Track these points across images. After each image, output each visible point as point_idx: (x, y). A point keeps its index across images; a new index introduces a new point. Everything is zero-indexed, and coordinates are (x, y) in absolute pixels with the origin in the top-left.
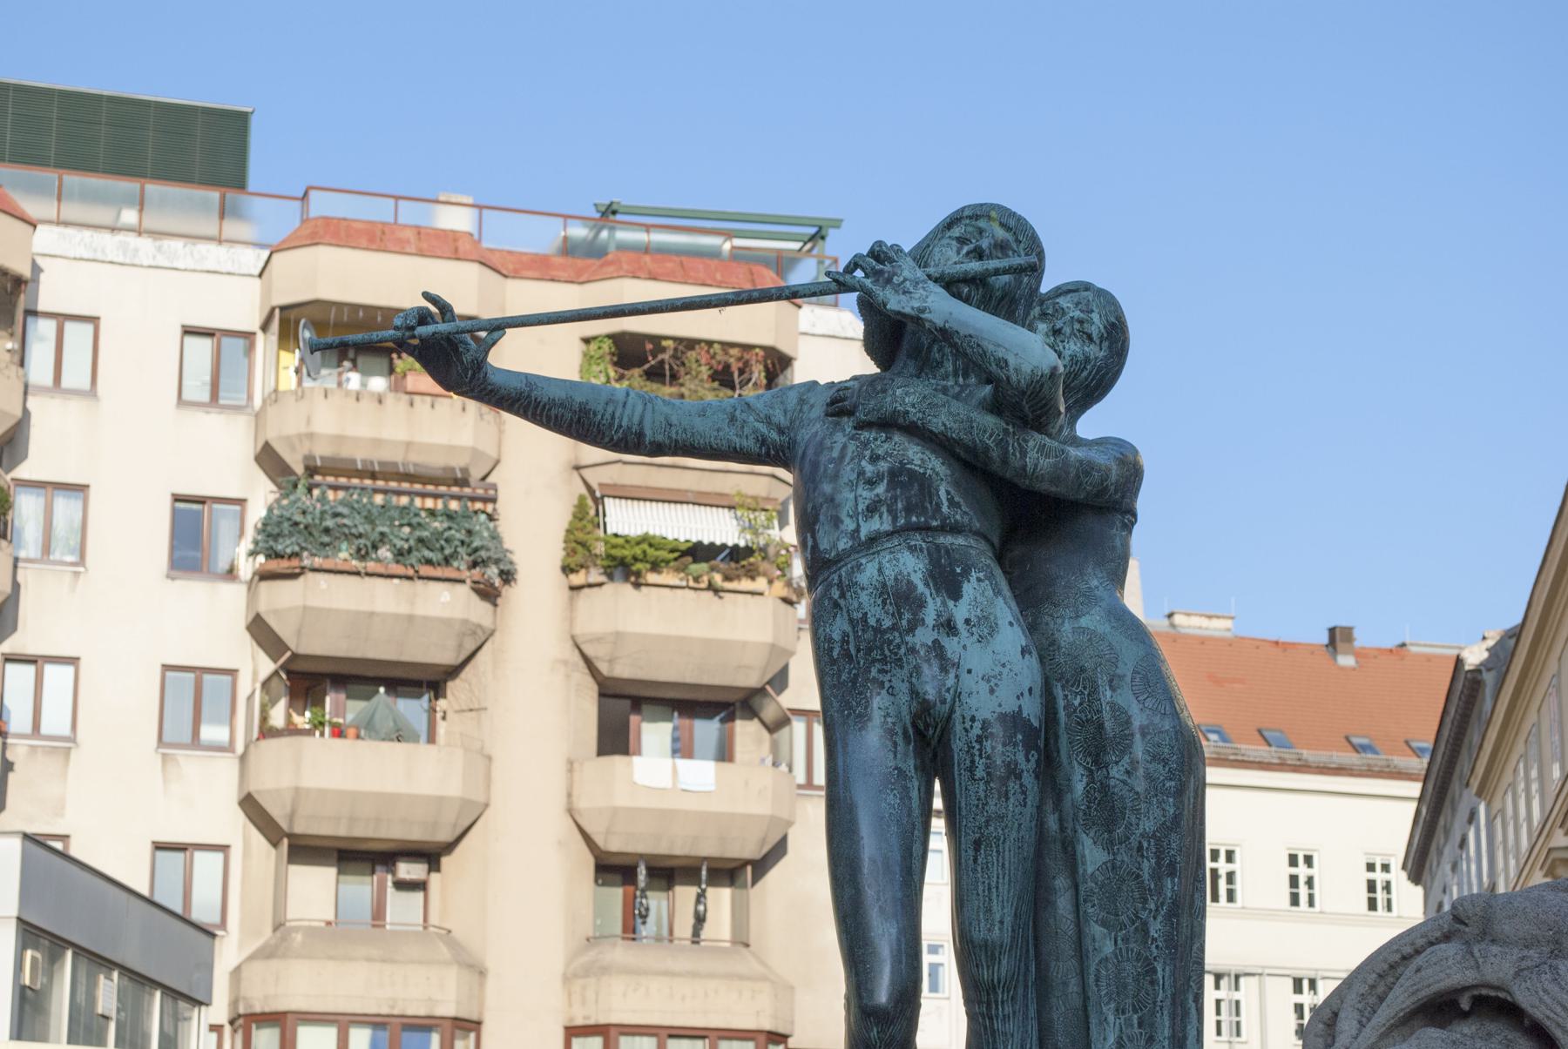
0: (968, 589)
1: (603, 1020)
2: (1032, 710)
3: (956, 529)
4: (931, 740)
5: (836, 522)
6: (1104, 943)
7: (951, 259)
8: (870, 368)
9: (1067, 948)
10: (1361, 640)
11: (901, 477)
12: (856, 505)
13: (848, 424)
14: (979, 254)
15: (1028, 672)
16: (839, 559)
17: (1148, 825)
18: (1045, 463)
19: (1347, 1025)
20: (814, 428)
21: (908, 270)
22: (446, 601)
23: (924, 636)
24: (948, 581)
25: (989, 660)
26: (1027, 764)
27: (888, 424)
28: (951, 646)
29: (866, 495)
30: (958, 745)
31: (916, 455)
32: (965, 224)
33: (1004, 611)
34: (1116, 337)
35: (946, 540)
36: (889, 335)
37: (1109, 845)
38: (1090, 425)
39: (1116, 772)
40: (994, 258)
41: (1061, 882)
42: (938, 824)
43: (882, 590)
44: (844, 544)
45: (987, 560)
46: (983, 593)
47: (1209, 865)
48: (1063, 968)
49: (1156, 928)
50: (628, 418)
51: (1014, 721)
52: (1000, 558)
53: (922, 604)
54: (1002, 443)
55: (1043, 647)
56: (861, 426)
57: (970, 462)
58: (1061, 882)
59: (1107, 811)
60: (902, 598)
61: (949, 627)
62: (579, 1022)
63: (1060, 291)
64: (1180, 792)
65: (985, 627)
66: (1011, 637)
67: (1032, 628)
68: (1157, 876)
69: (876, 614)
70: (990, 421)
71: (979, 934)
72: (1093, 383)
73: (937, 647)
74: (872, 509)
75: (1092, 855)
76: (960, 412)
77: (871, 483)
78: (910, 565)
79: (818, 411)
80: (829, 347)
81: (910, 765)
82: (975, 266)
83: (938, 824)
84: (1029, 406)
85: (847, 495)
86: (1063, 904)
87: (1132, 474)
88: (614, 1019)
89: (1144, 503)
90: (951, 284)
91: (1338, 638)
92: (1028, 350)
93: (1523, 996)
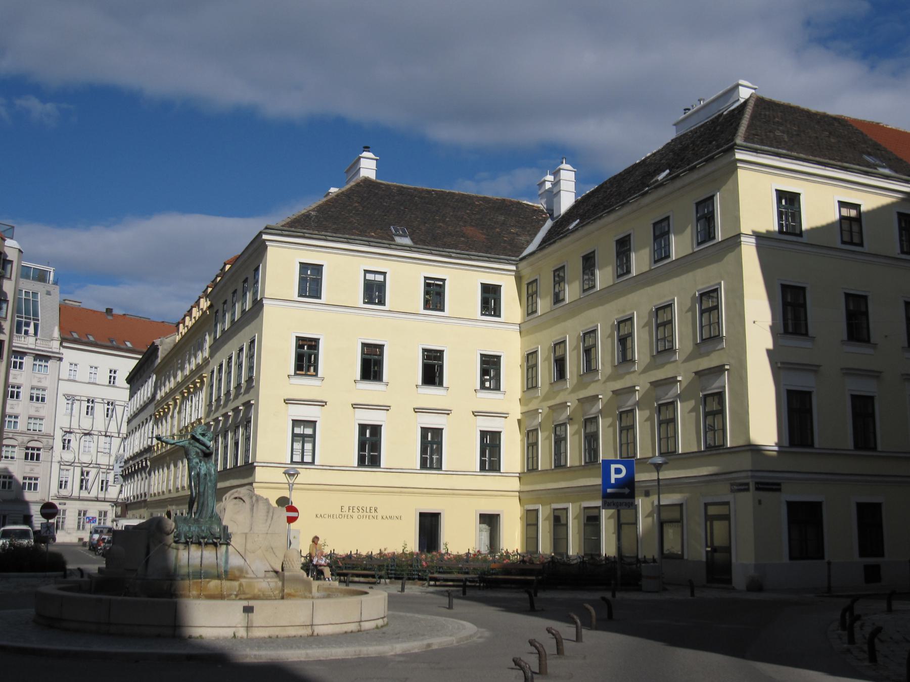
10: (115, 312)
91: (109, 311)
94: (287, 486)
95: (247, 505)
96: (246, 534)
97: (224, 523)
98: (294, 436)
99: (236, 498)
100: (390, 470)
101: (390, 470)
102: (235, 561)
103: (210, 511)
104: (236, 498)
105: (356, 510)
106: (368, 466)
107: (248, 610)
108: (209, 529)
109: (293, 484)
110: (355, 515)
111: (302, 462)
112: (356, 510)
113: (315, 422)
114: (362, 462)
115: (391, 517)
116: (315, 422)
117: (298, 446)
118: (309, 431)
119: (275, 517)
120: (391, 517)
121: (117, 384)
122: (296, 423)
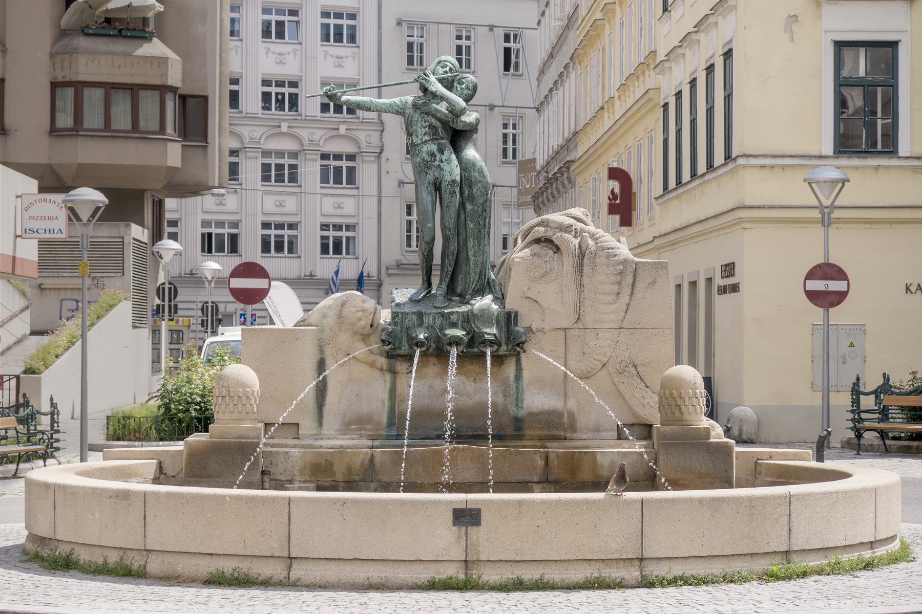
0: (445, 152)
1: (74, 79)
2: (458, 178)
3: (442, 138)
4: (437, 187)
6: (470, 225)
11: (431, 127)
13: (418, 112)
15: (457, 170)
17: (481, 201)
21: (433, 78)
23: (436, 163)
24: (441, 151)
25: (452, 170)
26: (458, 190)
28: (442, 165)
29: (424, 131)
30: (443, 186)
31: (434, 120)
33: (454, 156)
41: (462, 212)
44: (419, 142)
48: (462, 230)
49: (481, 223)
57: (444, 123)
58: (462, 212)
59: (472, 198)
60: (432, 155)
61: (441, 161)
62: (60, 79)
66: (455, 162)
69: (426, 158)
70: (450, 115)
74: (425, 134)
75: (469, 207)
78: (434, 147)
82: (446, 75)
86: (462, 217)
88: (81, 78)
94: (816, 214)
95: (569, 263)
96: (565, 329)
97: (510, 305)
99: (538, 241)
102: (537, 400)
103: (474, 276)
104: (538, 241)
107: (466, 517)
109: (833, 207)
119: (639, 286)
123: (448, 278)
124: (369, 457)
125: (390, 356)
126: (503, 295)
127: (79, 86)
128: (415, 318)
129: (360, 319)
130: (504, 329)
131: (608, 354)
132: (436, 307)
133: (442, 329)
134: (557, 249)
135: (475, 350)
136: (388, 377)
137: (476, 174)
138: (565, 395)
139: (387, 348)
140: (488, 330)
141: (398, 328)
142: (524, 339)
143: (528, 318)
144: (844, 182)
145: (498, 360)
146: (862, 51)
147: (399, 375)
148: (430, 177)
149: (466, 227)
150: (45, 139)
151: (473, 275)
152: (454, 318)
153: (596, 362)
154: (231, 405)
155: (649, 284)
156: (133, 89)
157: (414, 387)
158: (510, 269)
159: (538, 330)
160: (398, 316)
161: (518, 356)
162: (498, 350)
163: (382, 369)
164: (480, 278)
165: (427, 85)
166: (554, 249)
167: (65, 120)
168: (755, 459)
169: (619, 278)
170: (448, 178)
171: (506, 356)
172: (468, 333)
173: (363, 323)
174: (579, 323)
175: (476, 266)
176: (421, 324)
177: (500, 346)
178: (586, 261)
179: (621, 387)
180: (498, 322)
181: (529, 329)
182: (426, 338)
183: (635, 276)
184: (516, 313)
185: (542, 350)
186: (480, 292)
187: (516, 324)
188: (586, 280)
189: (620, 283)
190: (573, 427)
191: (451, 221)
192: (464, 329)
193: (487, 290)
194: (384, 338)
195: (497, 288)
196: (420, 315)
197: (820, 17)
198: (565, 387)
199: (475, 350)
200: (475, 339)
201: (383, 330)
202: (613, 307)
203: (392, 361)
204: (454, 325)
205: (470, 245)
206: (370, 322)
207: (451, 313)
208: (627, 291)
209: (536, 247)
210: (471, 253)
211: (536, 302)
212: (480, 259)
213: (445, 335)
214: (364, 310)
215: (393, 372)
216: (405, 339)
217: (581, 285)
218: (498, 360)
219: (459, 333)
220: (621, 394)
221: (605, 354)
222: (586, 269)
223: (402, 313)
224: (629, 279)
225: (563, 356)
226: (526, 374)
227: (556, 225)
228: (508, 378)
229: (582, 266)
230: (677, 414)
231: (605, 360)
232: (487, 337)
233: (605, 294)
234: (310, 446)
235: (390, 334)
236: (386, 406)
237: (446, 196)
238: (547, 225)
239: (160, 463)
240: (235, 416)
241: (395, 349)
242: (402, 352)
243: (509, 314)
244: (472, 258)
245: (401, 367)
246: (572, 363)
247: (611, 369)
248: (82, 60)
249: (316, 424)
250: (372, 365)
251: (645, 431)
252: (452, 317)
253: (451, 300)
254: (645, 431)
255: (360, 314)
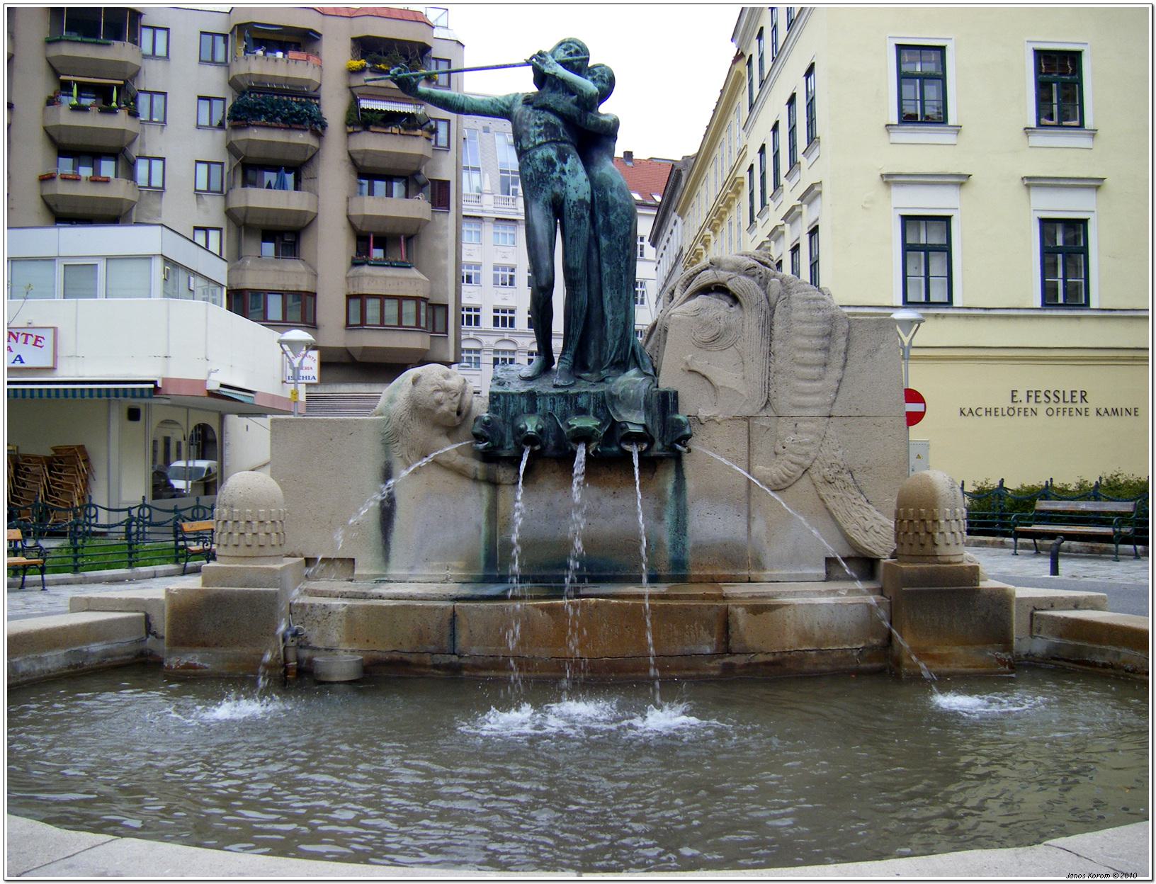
0: (569, 160)
2: (588, 198)
3: (565, 142)
4: (557, 208)
5: (528, 138)
6: (607, 269)
7: (562, 55)
8: (536, 90)
9: (595, 270)
11: (547, 124)
12: (534, 134)
14: (571, 54)
15: (587, 186)
16: (530, 149)
17: (621, 233)
18: (592, 122)
19: (677, 293)
20: (518, 108)
21: (550, 60)
22: (302, 138)
23: (556, 175)
25: (577, 184)
26: (587, 215)
27: (544, 108)
28: (564, 178)
29: (538, 130)
31: (553, 119)
32: (565, 44)
33: (580, 167)
34: (611, 82)
35: (562, 145)
36: (541, 78)
37: (609, 240)
38: (604, 108)
39: (612, 218)
40: (576, 57)
41: (594, 250)
42: (559, 230)
43: (543, 160)
45: (574, 151)
46: (574, 162)
47: (639, 243)
48: (594, 276)
50: (460, 103)
51: (582, 202)
52: (578, 151)
53: (555, 165)
54: (580, 116)
55: (591, 178)
56: (535, 108)
58: (594, 250)
59: (609, 229)
60: (550, 163)
61: (563, 172)
63: (595, 67)
64: (630, 224)
65: (574, 173)
66: (582, 175)
67: (587, 171)
68: (624, 249)
69: (541, 167)
71: (572, 265)
72: (605, 95)
73: (560, 178)
74: (540, 135)
75: (604, 242)
76: (566, 103)
77: (539, 127)
79: (520, 102)
80: (524, 83)
81: (551, 214)
83: (559, 230)
84: (590, 103)
85: (532, 130)
86: (595, 257)
87: (616, 124)
89: (619, 134)
90: (565, 64)
92: (589, 86)
93: (729, 285)
96: (747, 418)
97: (665, 383)
98: (907, 248)
99: (706, 290)
100: (1110, 314)
101: (1110, 314)
102: (711, 524)
103: (612, 342)
105: (1042, 398)
106: (1065, 306)
108: (604, 404)
110: (1042, 408)
111: (928, 303)
112: (1042, 398)
113: (947, 219)
114: (1049, 299)
115: (1115, 412)
116: (947, 219)
117: (917, 269)
118: (936, 239)
119: (856, 354)
120: (1115, 412)
121: (646, 256)
122: (908, 221)
123: (574, 345)
124: (448, 616)
125: (488, 457)
126: (654, 369)
127: (362, 298)
128: (524, 402)
129: (439, 403)
130: (657, 418)
131: (812, 455)
132: (556, 386)
133: (564, 417)
134: (735, 300)
135: (615, 449)
136: (485, 490)
137: (615, 195)
138: (749, 516)
139: (481, 446)
140: (634, 420)
141: (499, 417)
142: (687, 432)
143: (693, 404)
144: (919, 322)
145: (650, 464)
146: (923, 223)
147: (502, 488)
148: (545, 196)
149: (600, 272)
150: (343, 332)
151: (611, 341)
152: (582, 401)
153: (794, 467)
154: (236, 534)
155: (869, 351)
156: (400, 299)
157: (523, 508)
158: (666, 331)
159: (709, 420)
160: (498, 398)
161: (678, 458)
162: (648, 449)
163: (475, 480)
164: (620, 345)
165: (542, 67)
166: (730, 300)
167: (355, 320)
168: (1030, 609)
169: (826, 342)
170: (573, 196)
171: (660, 459)
172: (603, 425)
173: (445, 408)
174: (769, 409)
175: (615, 327)
176: (533, 410)
177: (651, 442)
178: (777, 317)
179: (831, 503)
180: (648, 407)
181: (696, 419)
182: (541, 432)
183: (848, 340)
184: (676, 393)
185: (715, 448)
186: (621, 365)
187: (676, 411)
188: (777, 346)
189: (827, 349)
190: (759, 564)
191: (578, 261)
192: (597, 416)
193: (632, 363)
194: (478, 430)
195: (647, 361)
196: (532, 396)
197: (889, 197)
198: (749, 503)
199: (615, 449)
200: (615, 432)
201: (476, 420)
202: (818, 385)
203: (493, 467)
204: (582, 412)
205: (607, 297)
206: (456, 407)
207: (578, 394)
208: (837, 360)
209: (701, 300)
210: (608, 309)
211: (704, 376)
212: (621, 317)
213: (570, 427)
214: (447, 390)
215: (493, 483)
216: (508, 434)
217: (771, 353)
218: (650, 464)
219: (590, 422)
220: (831, 515)
221: (807, 454)
222: (778, 329)
223: (505, 395)
224: (841, 343)
225: (745, 457)
226: (690, 484)
227: (731, 266)
228: (664, 491)
229: (772, 324)
230: (929, 546)
231: (807, 463)
232: (633, 429)
233: (805, 365)
234: (365, 596)
235: (486, 424)
236: (483, 532)
237: (570, 223)
238: (718, 267)
239: (147, 617)
240: (242, 551)
241: (494, 447)
242: (505, 454)
243: (665, 395)
244: (610, 317)
245: (503, 474)
246: (758, 468)
247: (817, 477)
248: (366, 280)
249: (380, 560)
250: (460, 472)
251: (866, 565)
252: (580, 400)
253: (580, 378)
254: (866, 565)
255: (439, 395)
